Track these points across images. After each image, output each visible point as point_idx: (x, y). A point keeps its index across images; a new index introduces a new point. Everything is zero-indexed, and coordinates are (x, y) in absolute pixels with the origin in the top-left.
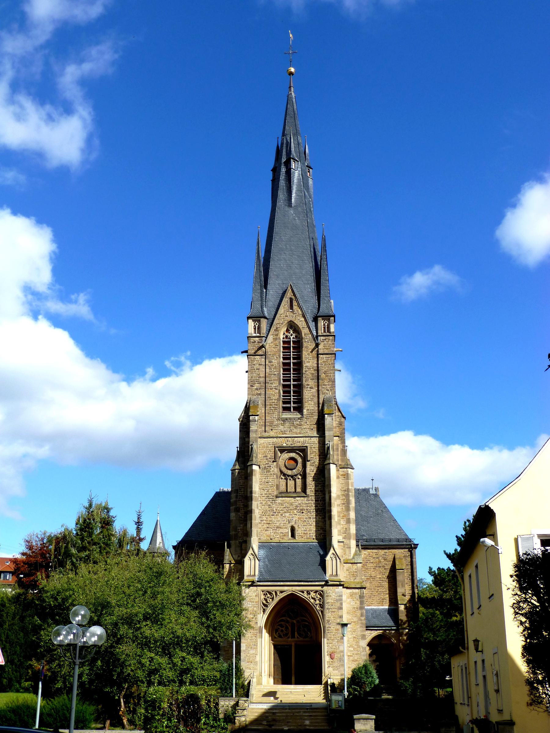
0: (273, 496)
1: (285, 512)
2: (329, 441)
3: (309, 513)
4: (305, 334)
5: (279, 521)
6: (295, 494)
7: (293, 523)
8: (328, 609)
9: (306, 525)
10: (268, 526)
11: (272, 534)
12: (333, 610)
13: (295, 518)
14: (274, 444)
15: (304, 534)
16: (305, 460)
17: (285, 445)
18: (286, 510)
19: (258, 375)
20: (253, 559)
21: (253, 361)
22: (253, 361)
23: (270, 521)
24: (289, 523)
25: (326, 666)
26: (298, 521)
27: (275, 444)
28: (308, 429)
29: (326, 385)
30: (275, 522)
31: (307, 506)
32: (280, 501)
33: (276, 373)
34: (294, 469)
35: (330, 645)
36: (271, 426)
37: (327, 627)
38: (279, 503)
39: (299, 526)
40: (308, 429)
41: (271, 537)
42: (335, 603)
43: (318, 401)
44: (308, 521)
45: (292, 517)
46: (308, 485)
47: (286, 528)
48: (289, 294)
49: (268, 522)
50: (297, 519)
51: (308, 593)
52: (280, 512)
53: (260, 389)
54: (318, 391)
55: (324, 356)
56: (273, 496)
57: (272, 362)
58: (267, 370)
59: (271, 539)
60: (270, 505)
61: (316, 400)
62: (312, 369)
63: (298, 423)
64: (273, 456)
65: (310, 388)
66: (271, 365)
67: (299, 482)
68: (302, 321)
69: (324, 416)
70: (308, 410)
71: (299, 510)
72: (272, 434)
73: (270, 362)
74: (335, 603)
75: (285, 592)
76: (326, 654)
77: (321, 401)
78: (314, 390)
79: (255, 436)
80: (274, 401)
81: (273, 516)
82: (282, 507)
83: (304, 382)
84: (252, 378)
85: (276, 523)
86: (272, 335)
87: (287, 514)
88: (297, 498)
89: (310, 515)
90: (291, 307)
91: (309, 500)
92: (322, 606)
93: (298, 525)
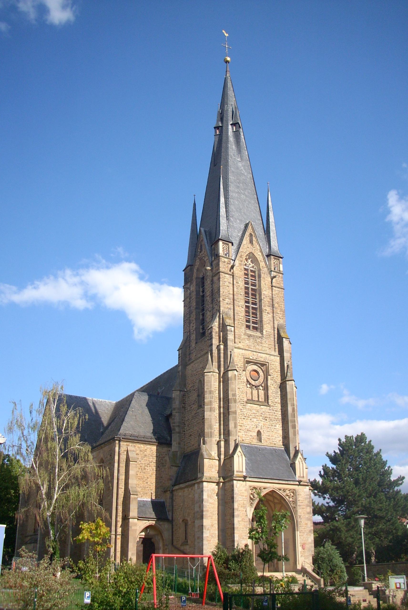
0: (243, 402)
1: (254, 418)
2: (289, 361)
3: (271, 421)
4: (262, 267)
5: (248, 425)
6: (258, 402)
7: (259, 428)
8: (299, 505)
9: (269, 431)
10: (240, 428)
11: (244, 436)
12: (303, 507)
13: (261, 425)
14: (242, 355)
15: (268, 439)
16: (267, 374)
17: (251, 358)
18: (254, 416)
19: (228, 291)
20: (241, 456)
21: (224, 278)
22: (224, 278)
23: (242, 424)
24: (256, 427)
25: (300, 555)
26: (263, 427)
27: (244, 356)
28: (267, 347)
29: (278, 313)
30: (246, 426)
31: (270, 415)
32: (249, 407)
33: (241, 293)
34: (257, 380)
35: (302, 537)
36: (240, 339)
37: (299, 521)
38: (248, 409)
39: (264, 432)
40: (267, 347)
41: (243, 439)
42: (304, 501)
43: (274, 326)
44: (271, 428)
45: (259, 423)
46: (269, 396)
47: (254, 431)
48: (249, 230)
49: (241, 425)
50: (262, 425)
51: (284, 490)
52: (249, 417)
53: (230, 304)
54: (273, 317)
55: (277, 289)
56: (243, 402)
57: (238, 283)
58: (235, 289)
59: (243, 440)
60: (241, 409)
61: (272, 323)
62: (268, 298)
63: (259, 340)
64: (242, 366)
65: (268, 313)
66: (238, 286)
67: (262, 392)
68: (259, 255)
69: (283, 339)
70: (266, 331)
71: (263, 417)
72: (240, 345)
73: (237, 283)
74: (304, 501)
75: (268, 489)
76: (299, 545)
77: (276, 326)
78: (271, 315)
79: (232, 344)
80: (241, 317)
81: (244, 420)
82: (251, 412)
83: (263, 307)
84: (224, 293)
85: (246, 427)
86: (238, 260)
87: (255, 420)
88: (261, 406)
89: (272, 423)
90: (251, 242)
91: (271, 410)
92: (295, 502)
93: (264, 431)
